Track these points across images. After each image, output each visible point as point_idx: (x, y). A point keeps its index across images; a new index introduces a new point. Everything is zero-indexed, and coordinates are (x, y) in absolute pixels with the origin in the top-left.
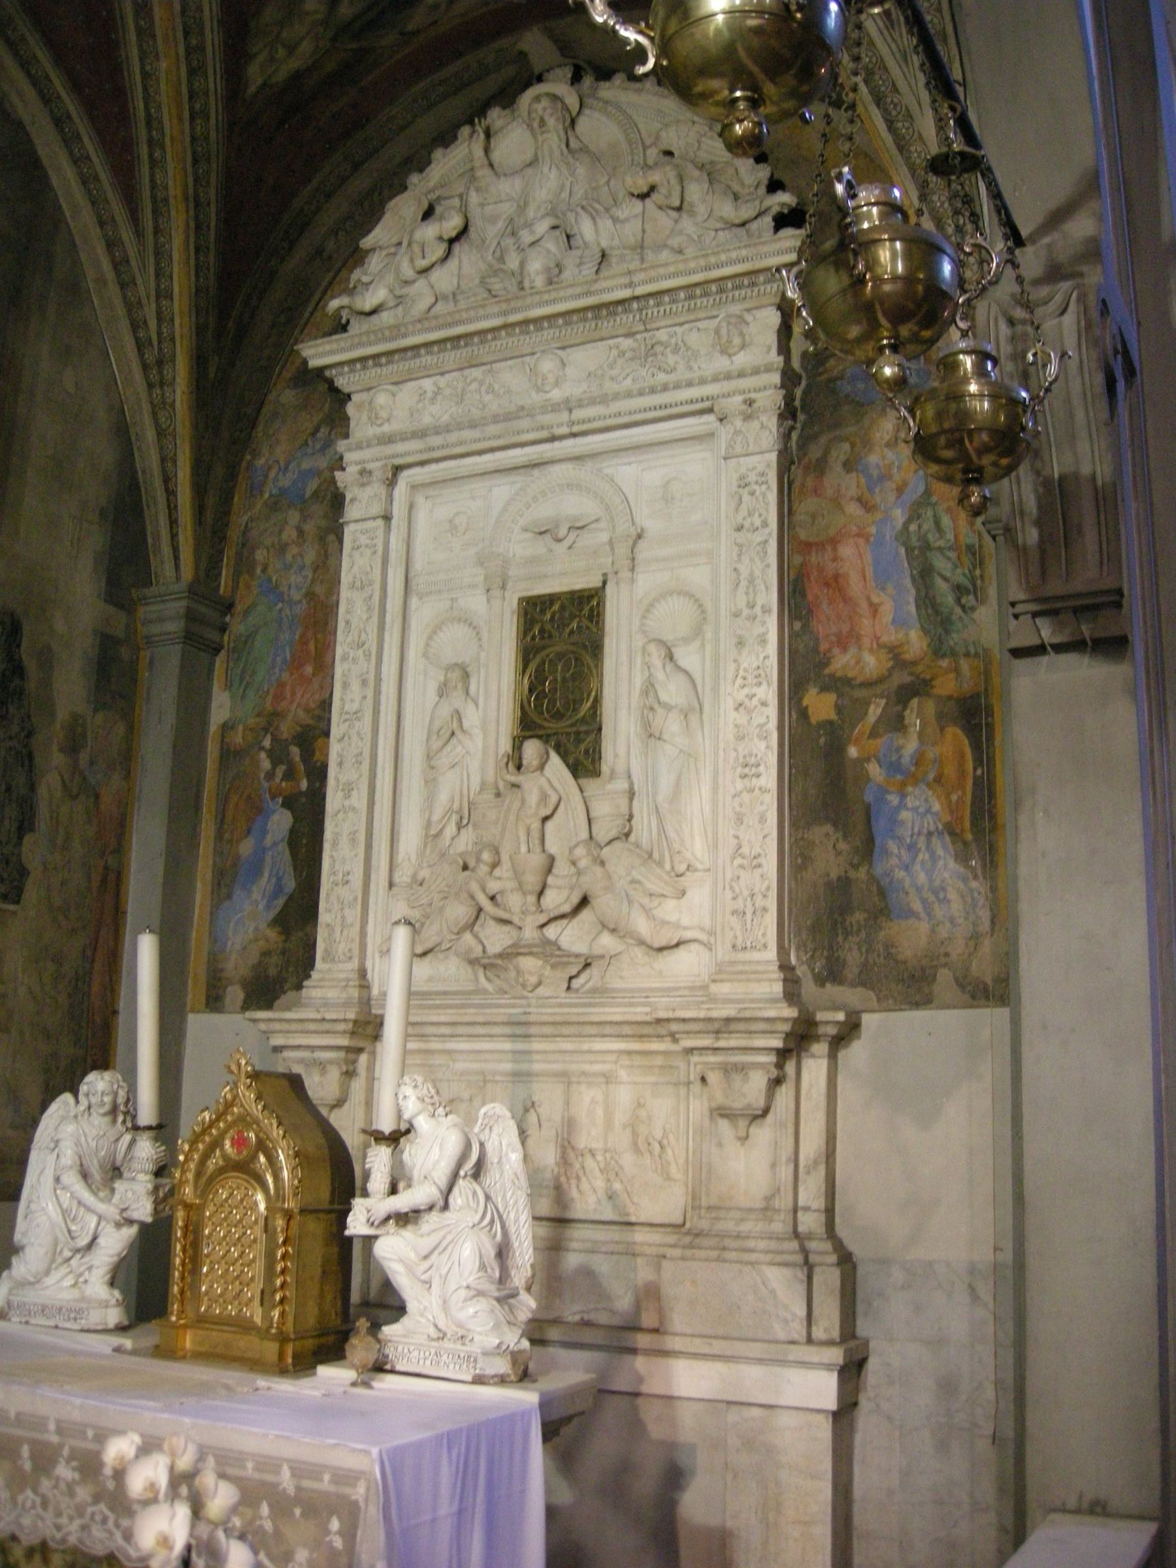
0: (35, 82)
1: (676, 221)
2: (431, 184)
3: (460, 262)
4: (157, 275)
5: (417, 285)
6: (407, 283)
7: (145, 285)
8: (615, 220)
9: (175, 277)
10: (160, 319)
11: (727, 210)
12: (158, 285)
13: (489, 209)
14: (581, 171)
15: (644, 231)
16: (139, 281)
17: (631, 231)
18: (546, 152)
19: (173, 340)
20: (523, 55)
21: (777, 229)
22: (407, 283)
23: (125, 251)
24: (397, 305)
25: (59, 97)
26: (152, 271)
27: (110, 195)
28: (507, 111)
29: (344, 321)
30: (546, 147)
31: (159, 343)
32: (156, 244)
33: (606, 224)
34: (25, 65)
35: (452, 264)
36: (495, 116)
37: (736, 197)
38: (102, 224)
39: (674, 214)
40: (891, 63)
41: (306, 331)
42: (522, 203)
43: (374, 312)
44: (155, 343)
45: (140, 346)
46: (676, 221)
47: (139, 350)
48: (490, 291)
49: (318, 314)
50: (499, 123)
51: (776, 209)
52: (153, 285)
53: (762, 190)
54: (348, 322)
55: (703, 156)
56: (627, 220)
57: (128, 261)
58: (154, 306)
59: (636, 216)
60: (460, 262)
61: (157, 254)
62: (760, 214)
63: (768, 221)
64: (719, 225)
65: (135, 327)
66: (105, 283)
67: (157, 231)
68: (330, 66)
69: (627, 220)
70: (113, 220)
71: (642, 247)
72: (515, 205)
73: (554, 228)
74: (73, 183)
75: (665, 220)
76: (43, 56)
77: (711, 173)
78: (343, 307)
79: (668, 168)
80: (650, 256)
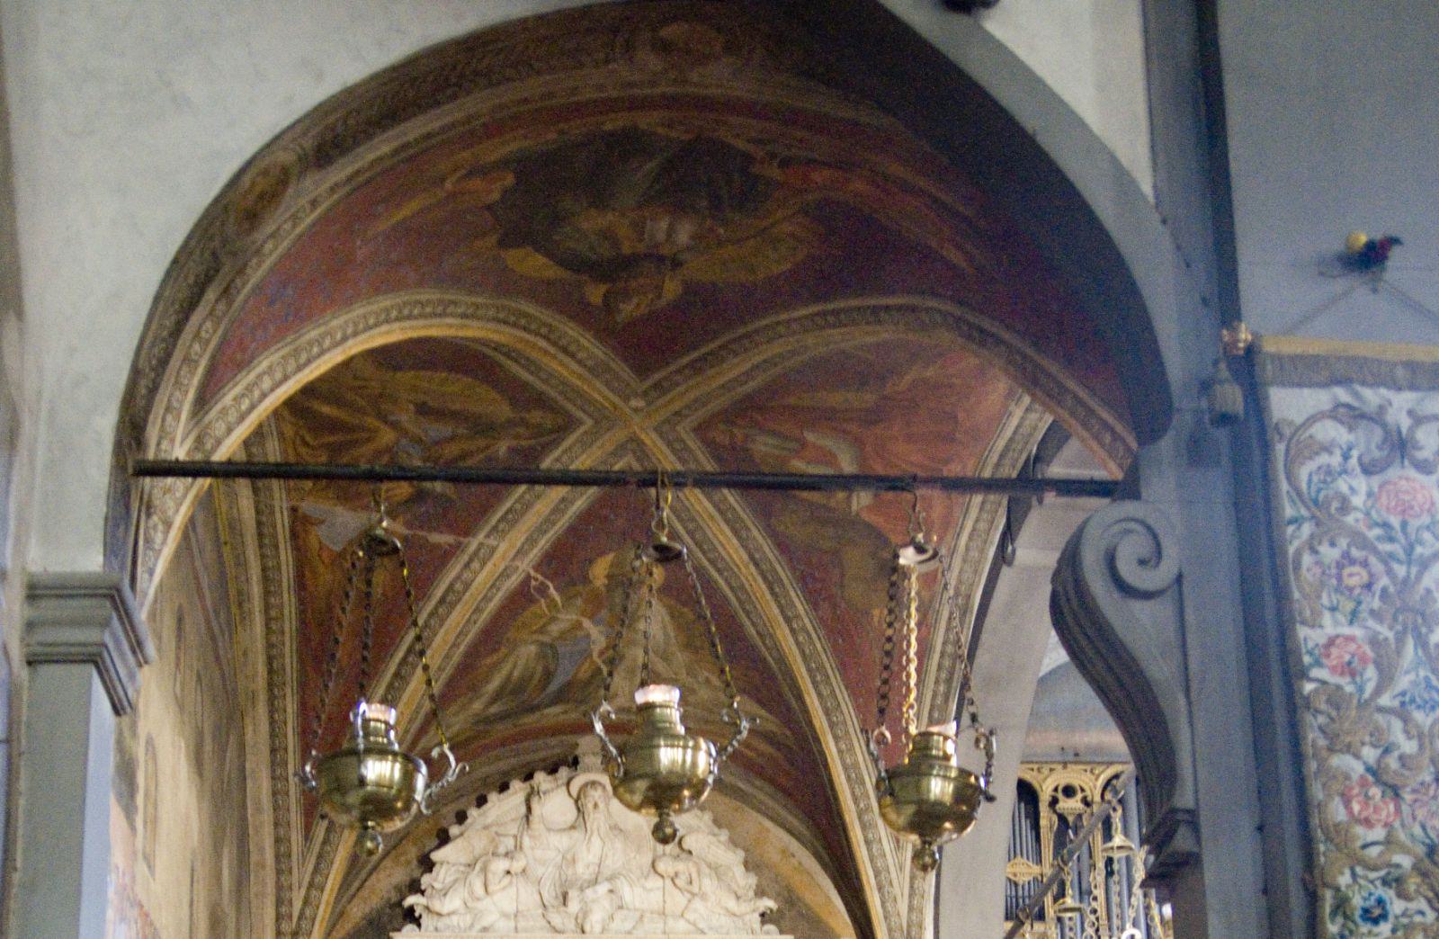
0: (272, 722)
1: (689, 901)
2: (489, 821)
3: (518, 890)
4: (316, 870)
5: (484, 902)
6: (478, 899)
7: (301, 875)
8: (644, 888)
9: (331, 877)
10: (306, 902)
11: (732, 904)
12: (312, 879)
13: (538, 853)
14: (619, 845)
15: (664, 902)
16: (295, 871)
17: (655, 899)
18: (595, 827)
19: (313, 920)
20: (577, 745)
21: (763, 923)
22: (478, 899)
23: (289, 848)
24: (466, 914)
25: (286, 736)
26: (310, 868)
27: (293, 807)
28: (550, 778)
29: (417, 914)
30: (595, 824)
31: (300, 918)
32: (322, 849)
33: (638, 890)
34: (272, 712)
35: (512, 891)
36: (540, 778)
37: (738, 898)
38: (276, 824)
39: (688, 896)
40: (892, 869)
41: (353, 903)
42: (569, 857)
43: (449, 914)
44: (295, 919)
45: (279, 918)
46: (689, 901)
47: (277, 920)
48: (549, 923)
49: (364, 893)
50: (544, 787)
51: (762, 909)
52: (307, 879)
53: (751, 894)
54: (420, 916)
55: (710, 858)
56: (651, 890)
57: (290, 856)
58: (303, 891)
59: (658, 889)
60: (518, 890)
61: (320, 856)
62: (754, 911)
63: (756, 918)
64: (722, 912)
65: (279, 902)
66: (264, 867)
67: (326, 842)
68: (462, 737)
69: (651, 890)
70: (289, 824)
71: (664, 914)
72: (560, 857)
73: (611, 891)
74: (264, 791)
75: (679, 900)
76: (291, 706)
77: (716, 870)
78: (418, 904)
79: (690, 864)
80: (671, 922)
